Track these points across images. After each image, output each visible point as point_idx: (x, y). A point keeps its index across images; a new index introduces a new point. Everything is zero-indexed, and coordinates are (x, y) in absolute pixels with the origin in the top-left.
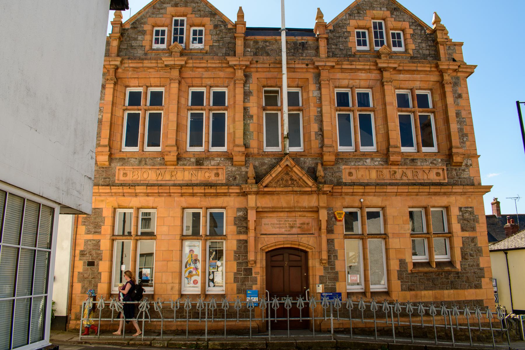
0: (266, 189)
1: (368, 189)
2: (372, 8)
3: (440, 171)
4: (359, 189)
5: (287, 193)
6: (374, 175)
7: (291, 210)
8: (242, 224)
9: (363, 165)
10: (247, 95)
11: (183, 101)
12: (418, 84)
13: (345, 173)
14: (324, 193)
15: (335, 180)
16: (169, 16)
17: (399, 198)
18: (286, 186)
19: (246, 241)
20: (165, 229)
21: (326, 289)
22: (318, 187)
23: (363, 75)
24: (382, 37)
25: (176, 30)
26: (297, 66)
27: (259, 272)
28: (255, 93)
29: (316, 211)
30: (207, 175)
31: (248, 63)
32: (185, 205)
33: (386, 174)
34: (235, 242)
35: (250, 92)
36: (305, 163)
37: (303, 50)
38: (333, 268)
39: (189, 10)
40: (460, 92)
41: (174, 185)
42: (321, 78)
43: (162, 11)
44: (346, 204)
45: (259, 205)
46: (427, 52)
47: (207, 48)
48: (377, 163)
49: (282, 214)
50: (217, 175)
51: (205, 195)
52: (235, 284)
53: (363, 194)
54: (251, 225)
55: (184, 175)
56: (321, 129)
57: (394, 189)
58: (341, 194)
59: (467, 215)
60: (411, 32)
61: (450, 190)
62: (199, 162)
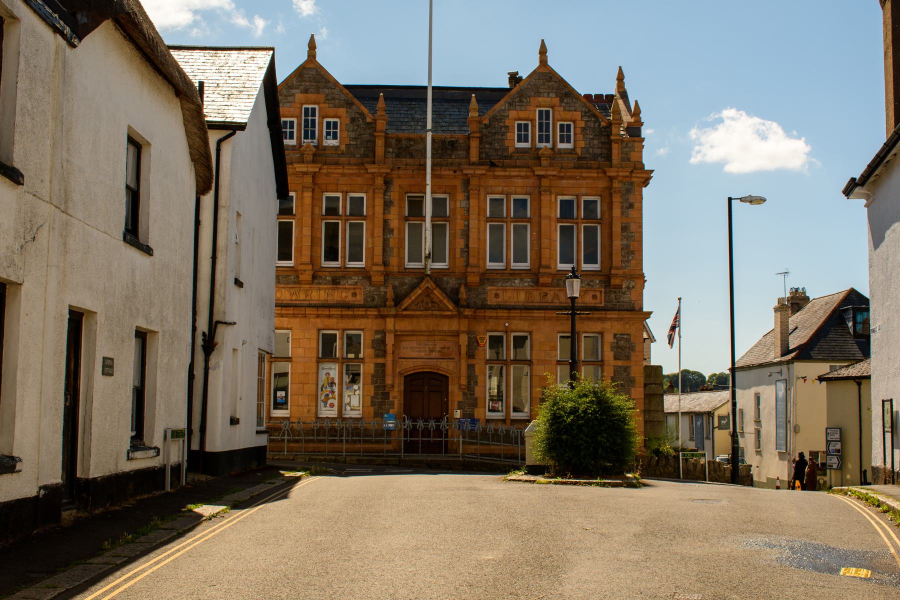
0: (404, 313)
1: (513, 313)
2: (538, 94)
3: (598, 294)
4: (503, 313)
5: (426, 316)
6: (522, 297)
7: (431, 334)
8: (379, 346)
9: (511, 286)
10: (387, 205)
11: (317, 211)
12: (583, 190)
13: (492, 294)
14: (466, 317)
15: (479, 303)
16: (298, 106)
17: (548, 323)
18: (427, 309)
19: (384, 365)
20: (300, 351)
21: (464, 415)
22: (459, 312)
23: (519, 181)
24: (547, 130)
25: (306, 121)
26: (443, 173)
27: (396, 396)
28: (396, 203)
29: (457, 334)
30: (344, 295)
31: (389, 171)
32: (321, 326)
33: (536, 297)
34: (372, 366)
35: (391, 202)
36: (448, 283)
37: (452, 151)
38: (473, 394)
39: (321, 97)
40: (631, 201)
41: (310, 306)
42: (471, 187)
43: (290, 99)
44: (489, 328)
45: (397, 328)
46: (599, 151)
47: (343, 147)
48: (526, 284)
49: (422, 338)
50: (354, 295)
51: (342, 317)
52: (372, 408)
53: (508, 318)
54: (389, 349)
55: (319, 295)
56: (467, 246)
57: (541, 314)
58: (485, 317)
59: (622, 343)
60: (583, 124)
61: (603, 316)
62: (335, 282)
